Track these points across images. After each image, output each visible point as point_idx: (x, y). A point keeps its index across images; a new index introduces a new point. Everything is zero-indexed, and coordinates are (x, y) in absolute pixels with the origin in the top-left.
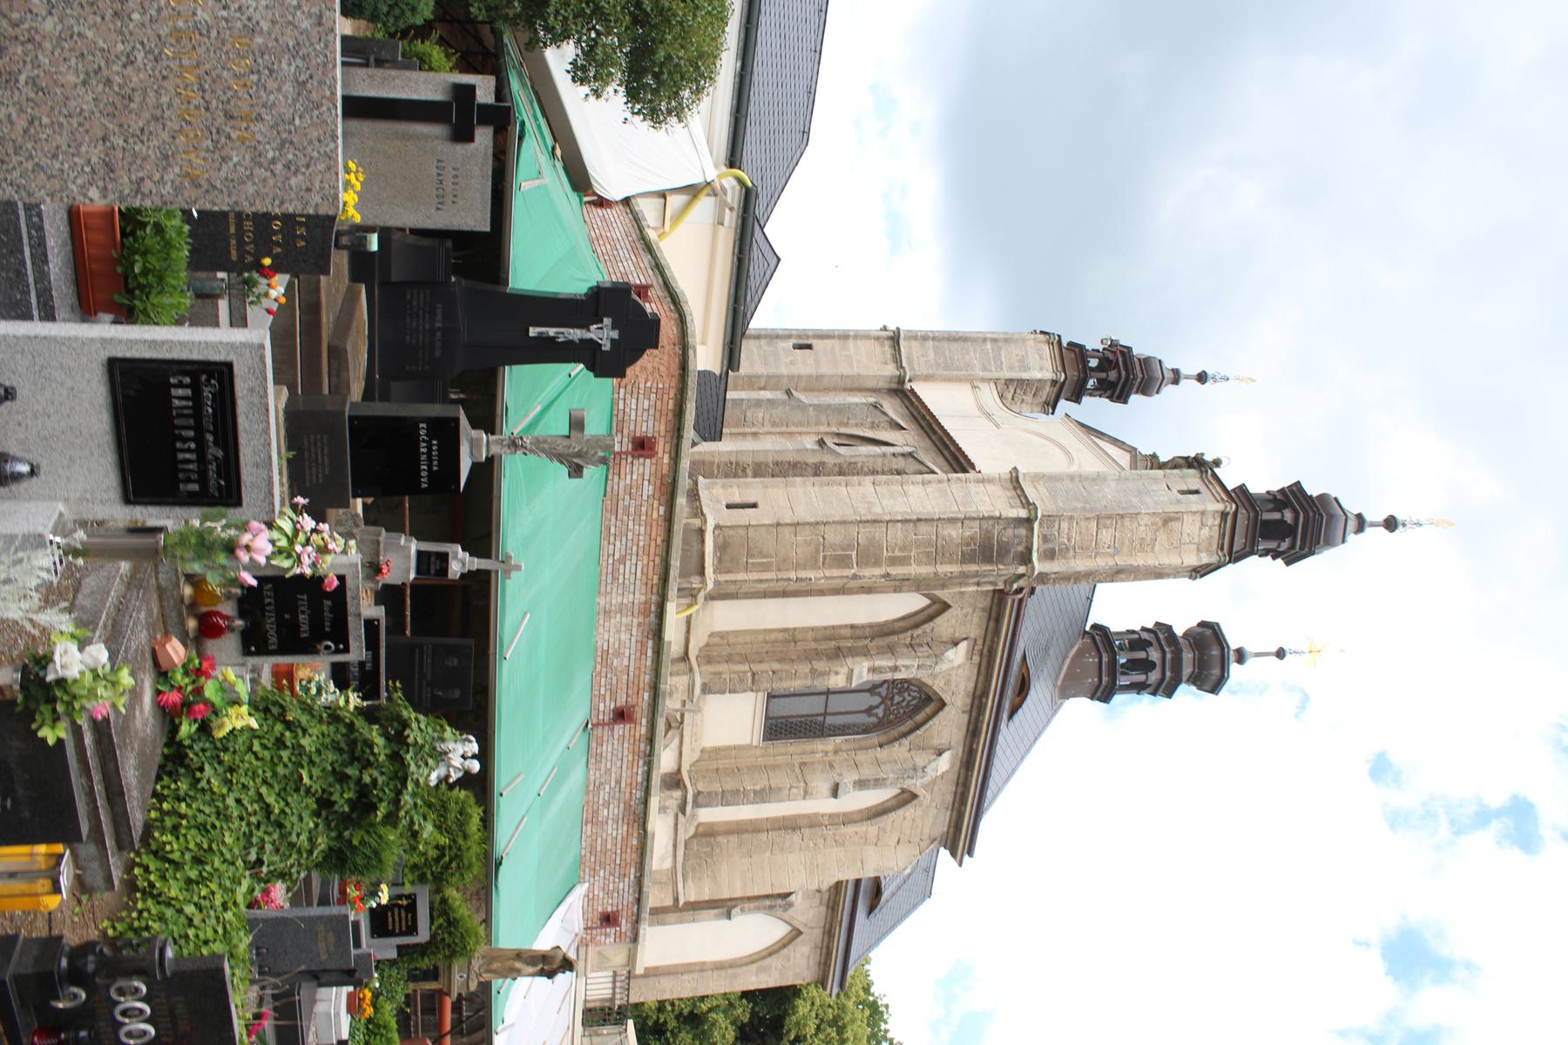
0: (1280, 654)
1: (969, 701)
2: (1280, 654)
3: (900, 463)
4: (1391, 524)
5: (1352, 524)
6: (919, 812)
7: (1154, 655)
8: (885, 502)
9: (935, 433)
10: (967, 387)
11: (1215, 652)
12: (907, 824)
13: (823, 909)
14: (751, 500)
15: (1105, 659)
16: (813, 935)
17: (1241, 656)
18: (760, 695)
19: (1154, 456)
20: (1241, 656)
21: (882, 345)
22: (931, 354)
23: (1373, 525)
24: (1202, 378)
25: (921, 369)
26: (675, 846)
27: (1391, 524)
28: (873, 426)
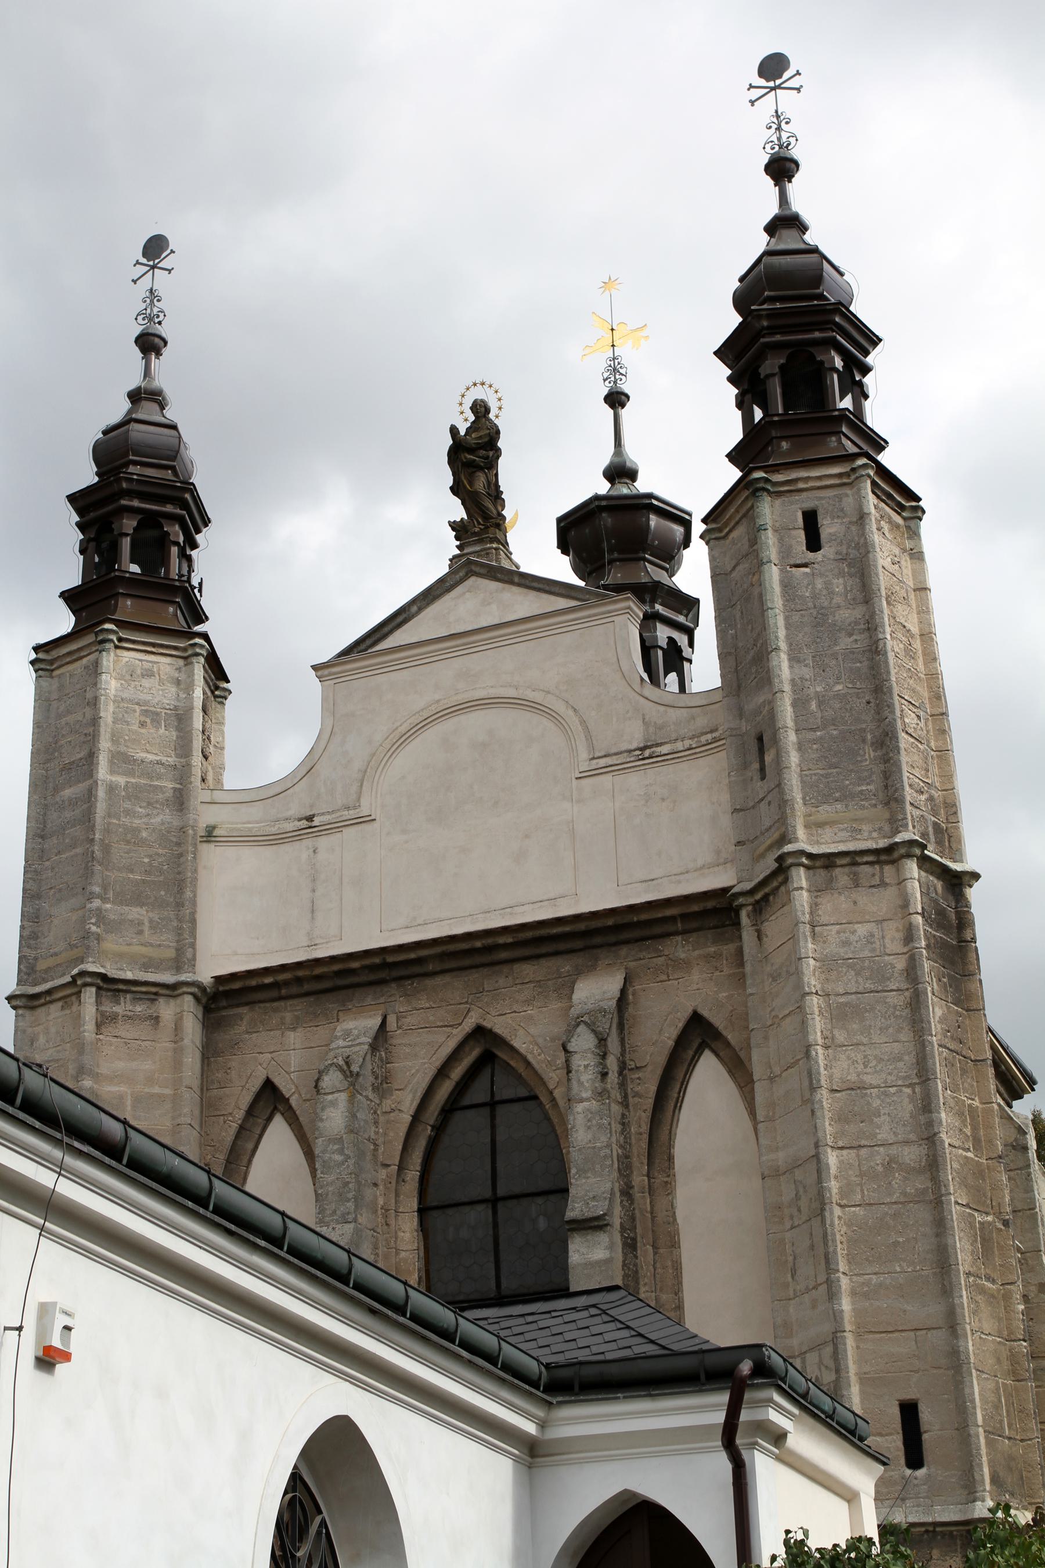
0: (616, 400)
2: (616, 400)
3: (612, 1063)
4: (781, 169)
5: (788, 240)
8: (883, 1135)
9: (419, 961)
10: (211, 856)
14: (895, 1413)
17: (620, 472)
19: (459, 529)
20: (620, 472)
21: (114, 1018)
22: (135, 912)
24: (150, 344)
25: (164, 945)
27: (781, 169)
28: (383, 1084)
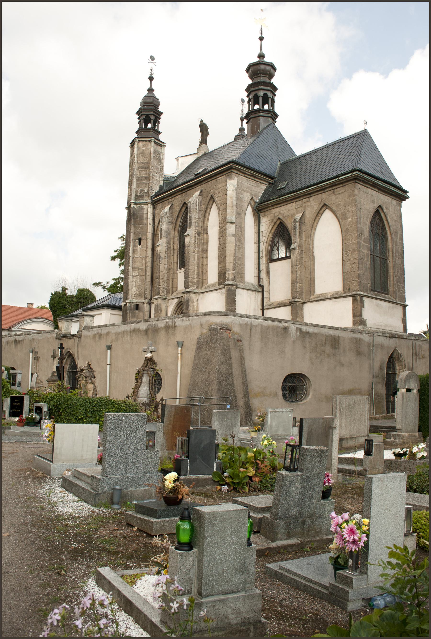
0: (261, 39)
1: (184, 194)
2: (261, 39)
4: (151, 79)
6: (217, 192)
7: (261, 93)
11: (262, 67)
12: (220, 195)
13: (311, 199)
15: (261, 114)
16: (326, 197)
17: (261, 56)
18: (178, 272)
20: (261, 56)
23: (151, 83)
26: (217, 290)
27: (151, 79)
